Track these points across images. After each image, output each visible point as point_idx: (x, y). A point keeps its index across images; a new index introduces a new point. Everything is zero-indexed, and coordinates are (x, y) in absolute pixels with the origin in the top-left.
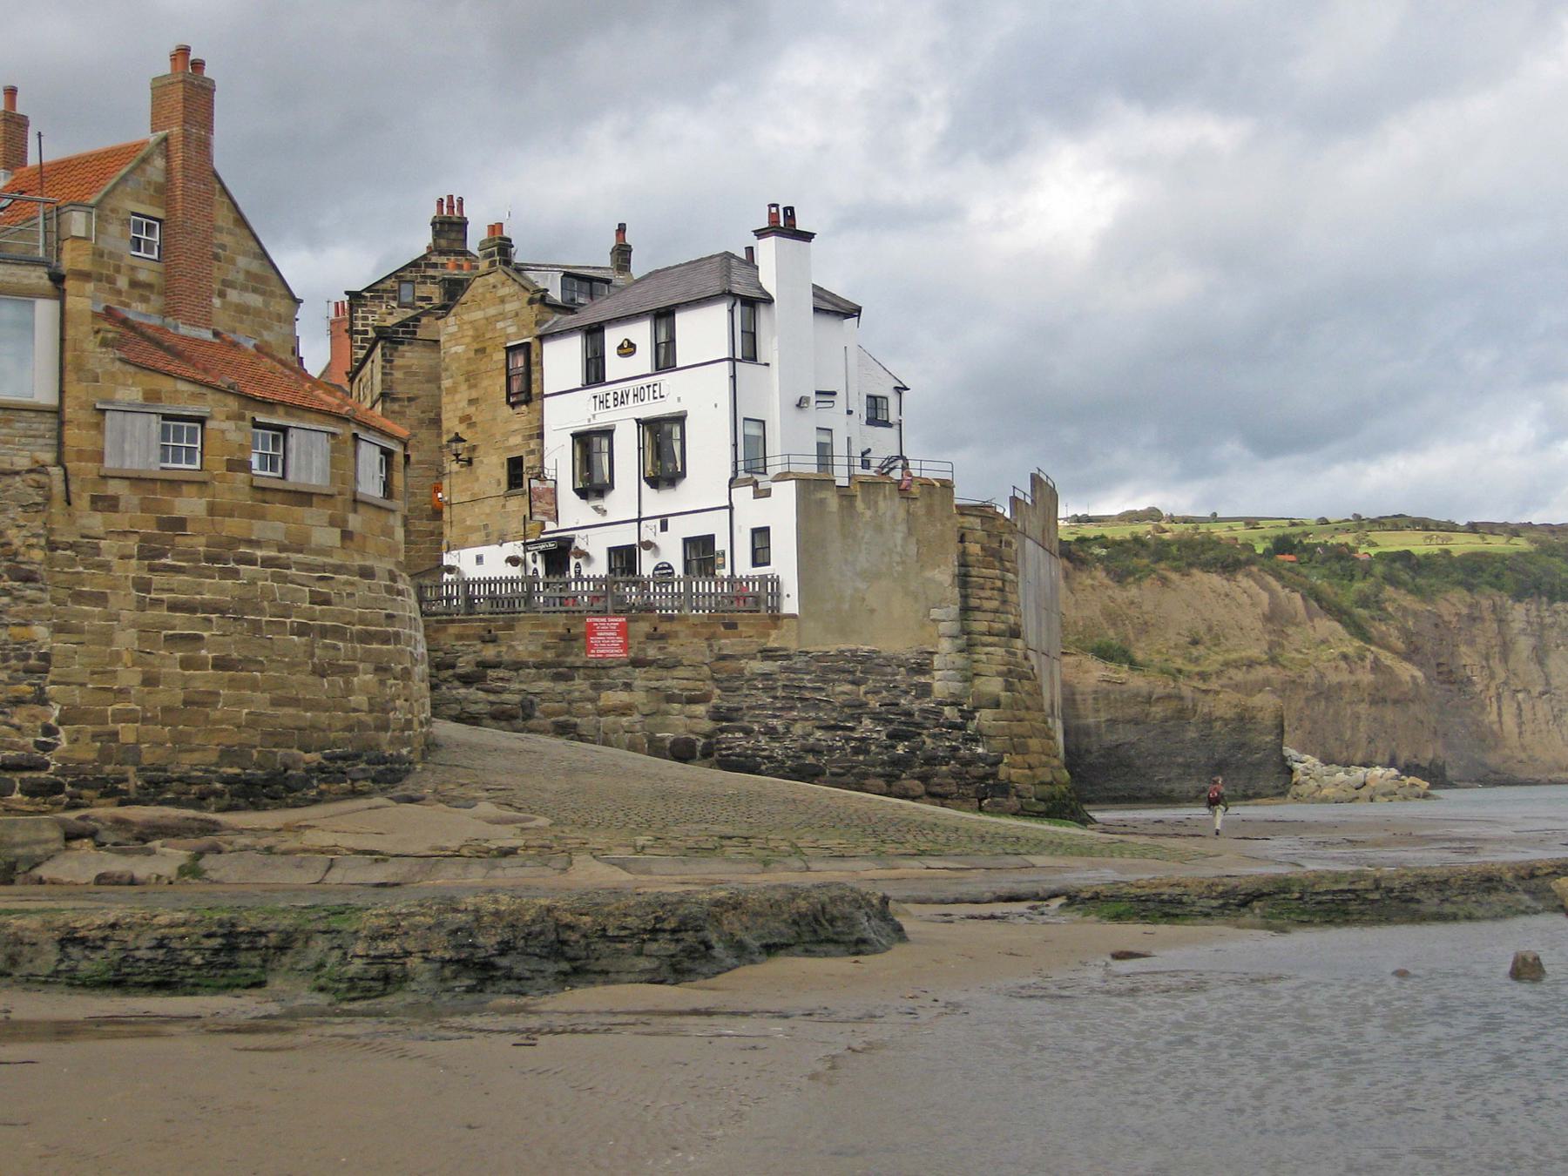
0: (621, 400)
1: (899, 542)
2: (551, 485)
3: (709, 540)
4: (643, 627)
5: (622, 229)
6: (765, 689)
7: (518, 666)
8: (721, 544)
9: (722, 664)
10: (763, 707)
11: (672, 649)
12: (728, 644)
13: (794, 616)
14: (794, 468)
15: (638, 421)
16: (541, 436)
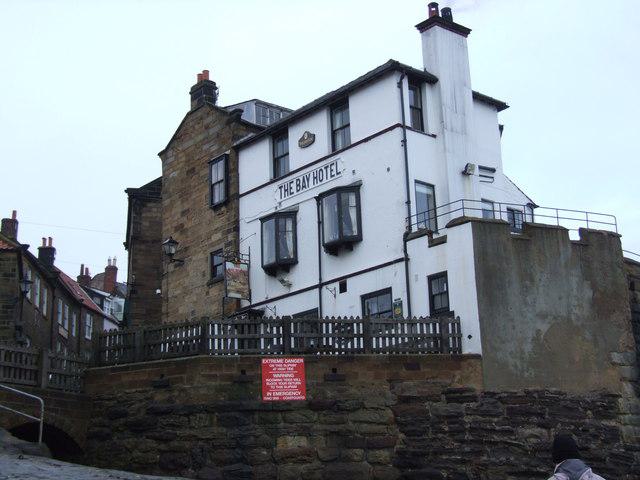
0: (302, 185)
1: (575, 286)
2: (244, 267)
4: (323, 370)
6: (452, 433)
7: (191, 411)
8: (399, 294)
9: (404, 407)
10: (451, 452)
11: (353, 390)
12: (412, 386)
13: (477, 357)
14: (469, 214)
16: (237, 229)
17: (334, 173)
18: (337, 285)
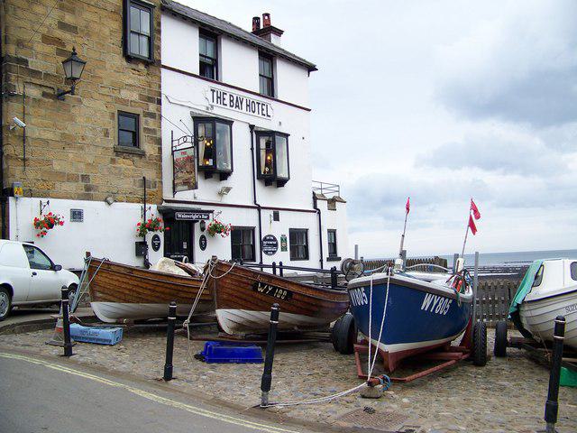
3: (306, 231)
15: (252, 127)
16: (159, 102)
18: (271, 212)
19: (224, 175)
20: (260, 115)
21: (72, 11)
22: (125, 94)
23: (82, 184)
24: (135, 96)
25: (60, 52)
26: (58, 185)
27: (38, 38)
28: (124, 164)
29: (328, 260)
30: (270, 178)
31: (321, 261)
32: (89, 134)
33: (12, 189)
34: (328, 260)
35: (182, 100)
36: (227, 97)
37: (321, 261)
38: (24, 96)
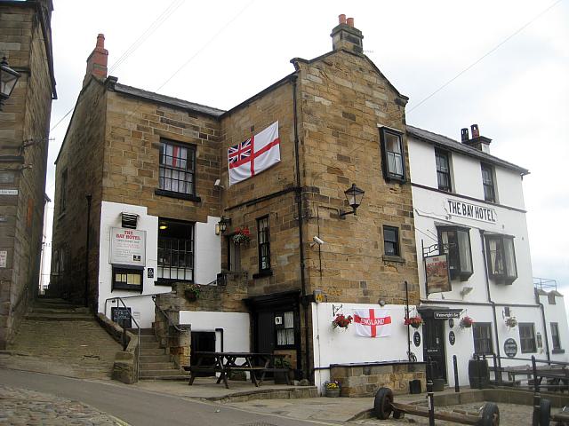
3: (533, 324)
5: (101, 38)
8: (538, 329)
16: (412, 216)
17: (490, 218)
18: (503, 308)
19: (465, 277)
20: (487, 220)
21: (345, 145)
22: (388, 211)
23: (361, 290)
24: (394, 212)
25: (342, 180)
26: (344, 291)
27: (324, 169)
28: (390, 271)
29: (554, 352)
30: (501, 276)
31: (548, 353)
32: (364, 247)
33: (313, 296)
34: (554, 352)
35: (429, 210)
36: (460, 206)
37: (548, 353)
38: (318, 217)
